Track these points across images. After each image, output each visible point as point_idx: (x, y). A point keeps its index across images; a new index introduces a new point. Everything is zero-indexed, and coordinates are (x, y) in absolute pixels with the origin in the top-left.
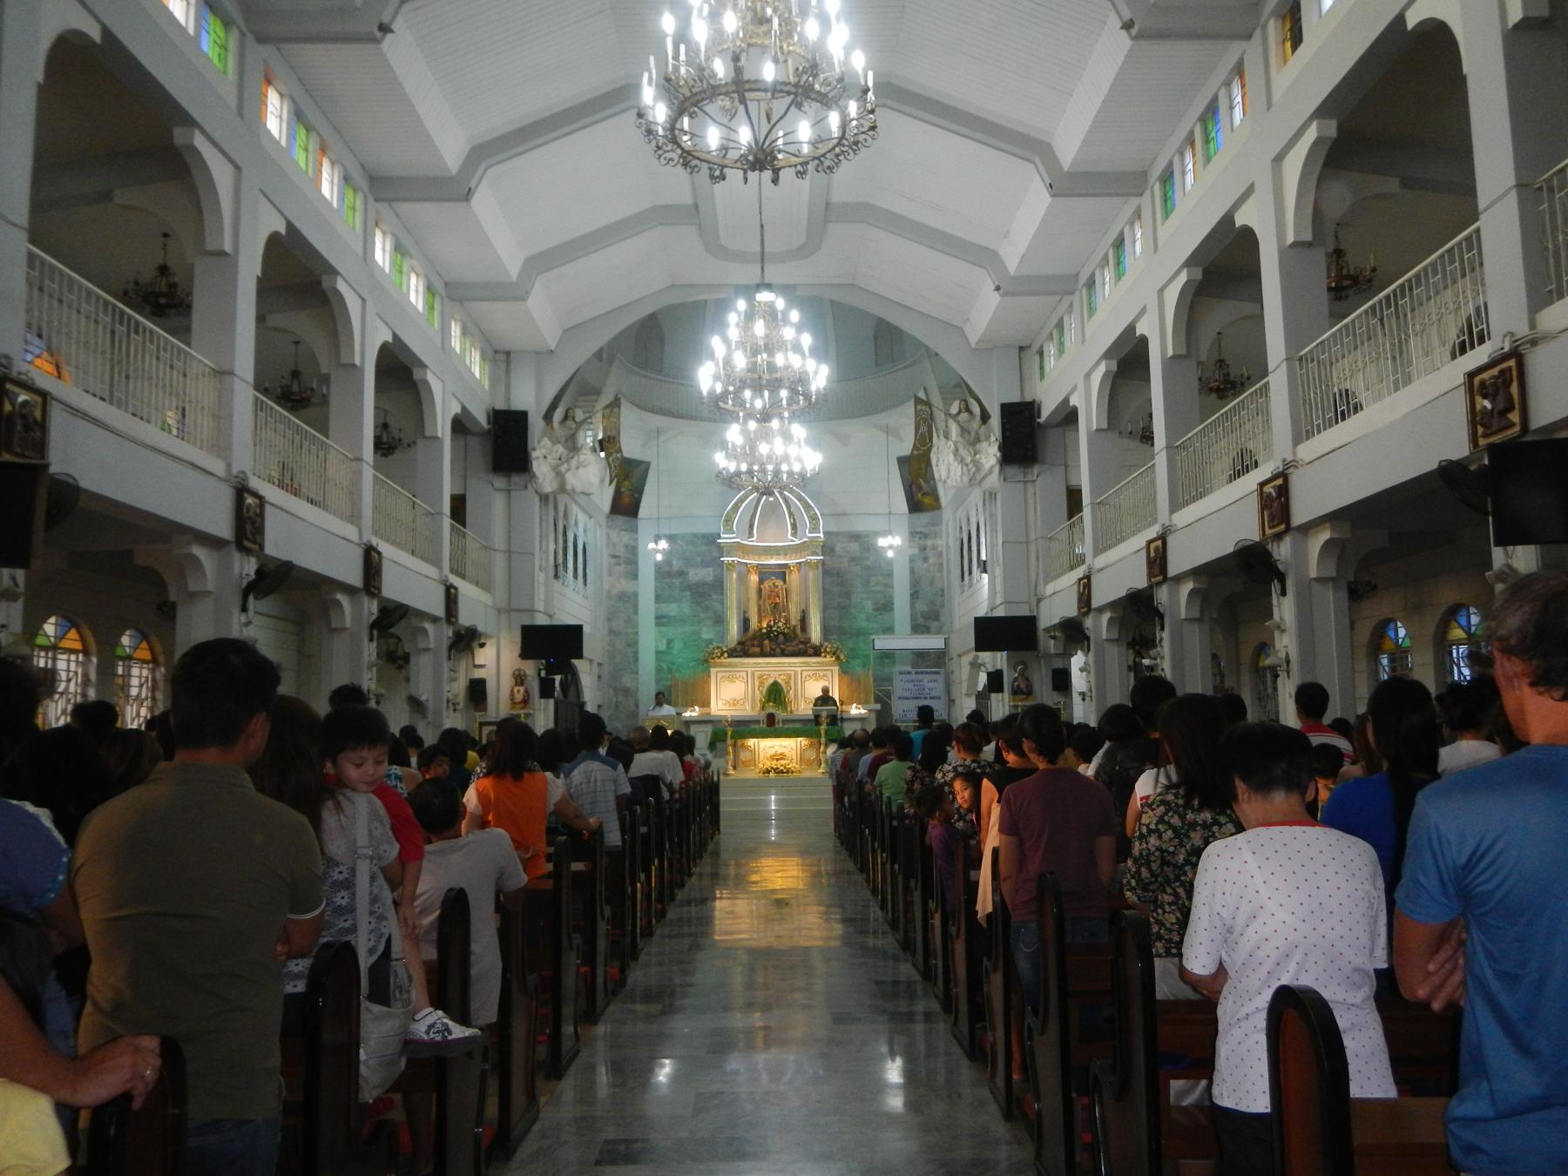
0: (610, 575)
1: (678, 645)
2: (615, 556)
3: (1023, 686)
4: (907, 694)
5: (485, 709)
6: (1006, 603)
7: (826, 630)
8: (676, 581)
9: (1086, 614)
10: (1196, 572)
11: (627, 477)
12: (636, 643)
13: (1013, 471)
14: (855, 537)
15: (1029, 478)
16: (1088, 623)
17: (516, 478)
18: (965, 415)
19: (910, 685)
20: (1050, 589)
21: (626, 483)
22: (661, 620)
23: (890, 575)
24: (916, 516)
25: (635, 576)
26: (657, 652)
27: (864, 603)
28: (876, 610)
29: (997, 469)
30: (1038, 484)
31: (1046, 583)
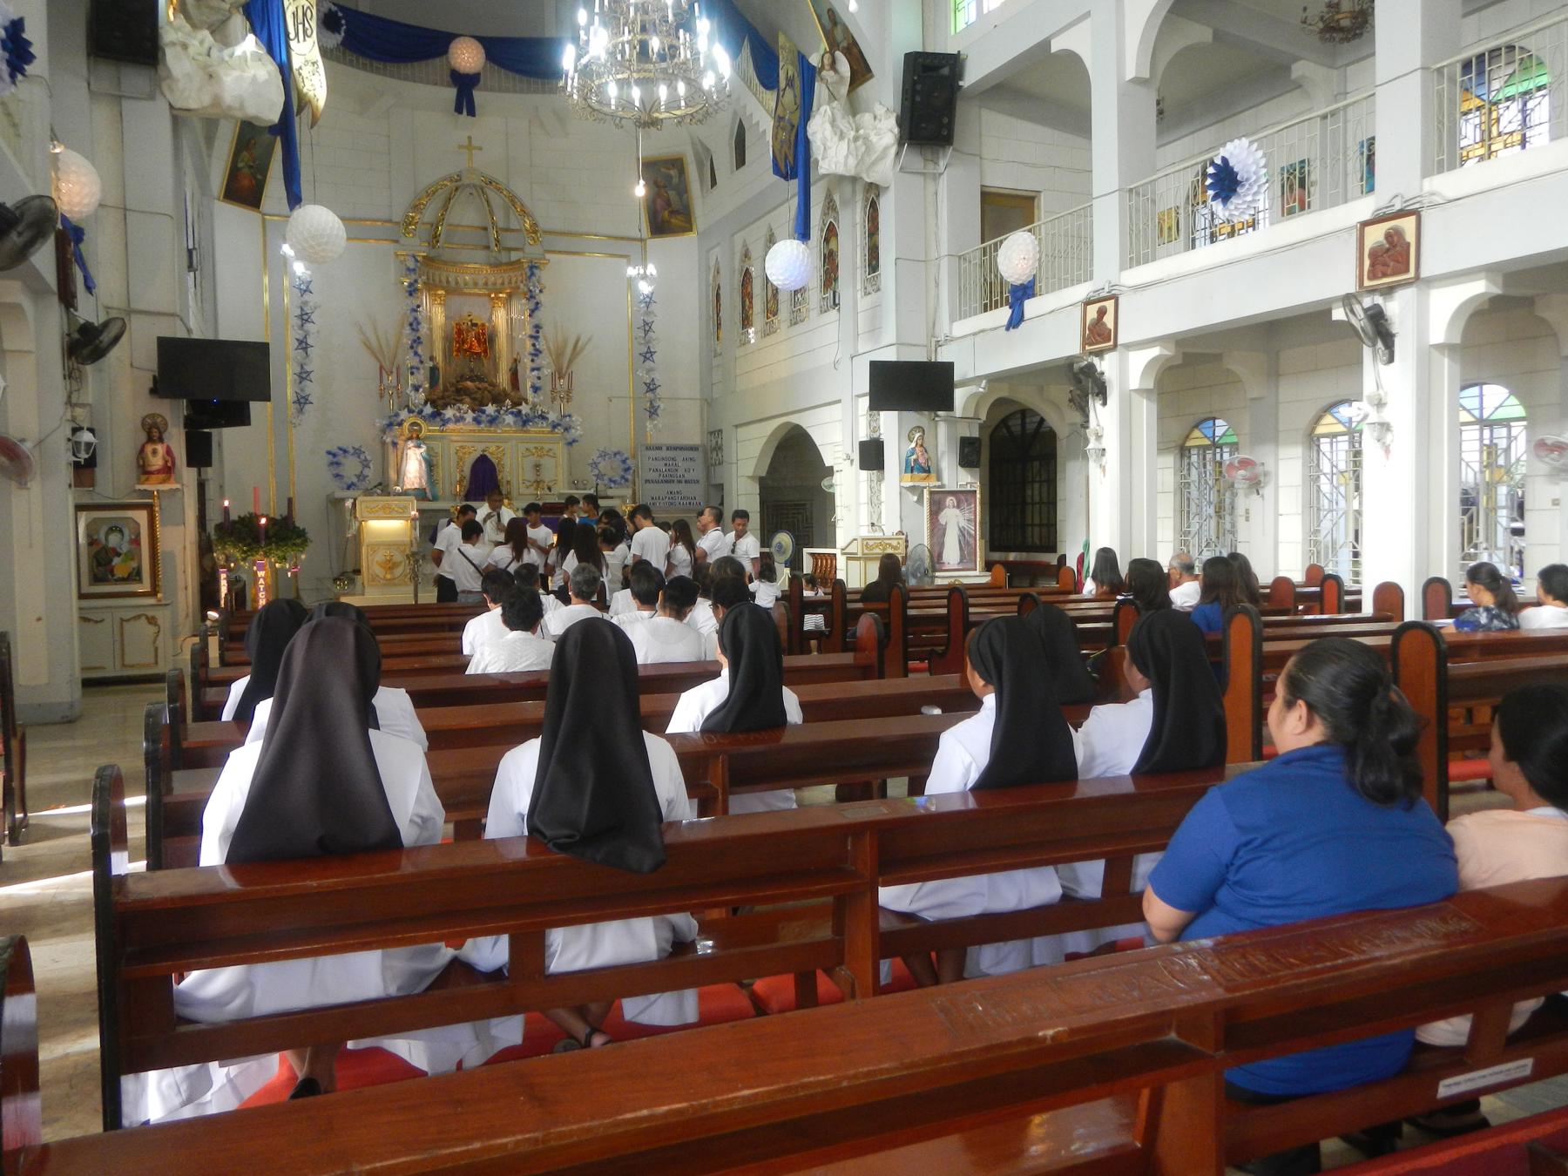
3: (921, 460)
4: (654, 476)
5: (92, 483)
6: (899, 344)
9: (1100, 354)
10: (1489, 270)
13: (915, 160)
15: (930, 168)
16: (1107, 366)
17: (135, 79)
18: (828, 74)
19: (660, 465)
20: (962, 327)
29: (893, 150)
30: (943, 182)
31: (952, 320)
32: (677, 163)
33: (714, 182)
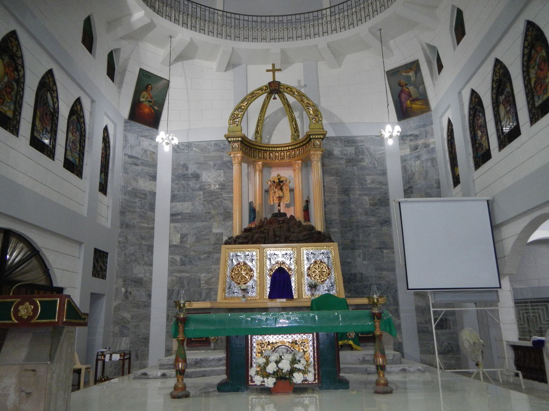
0: (126, 171)
1: (191, 239)
2: (130, 157)
7: (327, 222)
8: (192, 183)
11: (146, 88)
12: (152, 237)
14: (349, 141)
21: (145, 93)
22: (175, 217)
23: (384, 173)
24: (403, 121)
25: (154, 178)
26: (171, 246)
27: (362, 201)
28: (375, 205)
32: (414, 66)
33: (440, 67)
